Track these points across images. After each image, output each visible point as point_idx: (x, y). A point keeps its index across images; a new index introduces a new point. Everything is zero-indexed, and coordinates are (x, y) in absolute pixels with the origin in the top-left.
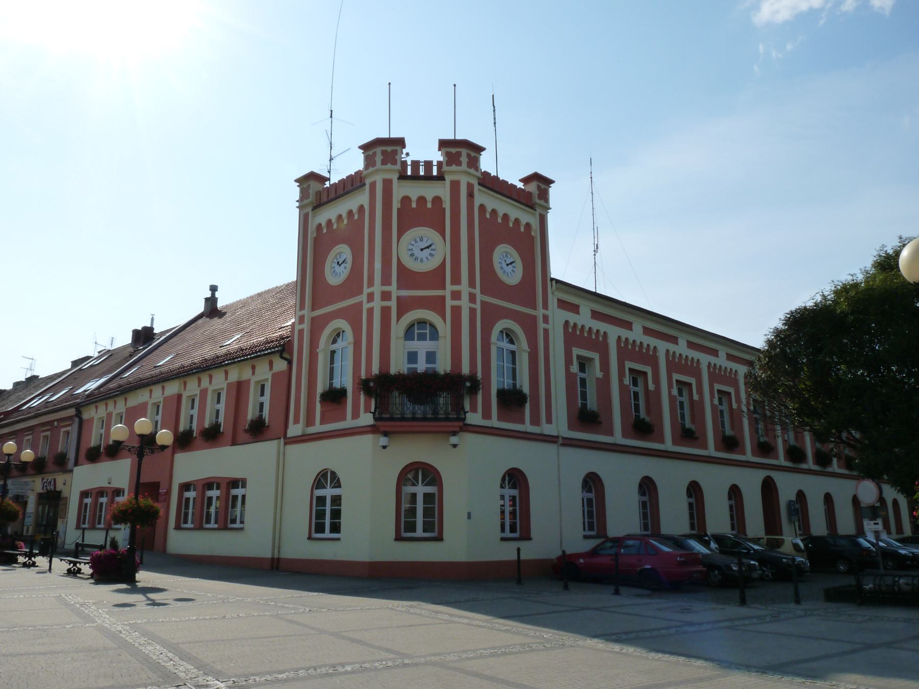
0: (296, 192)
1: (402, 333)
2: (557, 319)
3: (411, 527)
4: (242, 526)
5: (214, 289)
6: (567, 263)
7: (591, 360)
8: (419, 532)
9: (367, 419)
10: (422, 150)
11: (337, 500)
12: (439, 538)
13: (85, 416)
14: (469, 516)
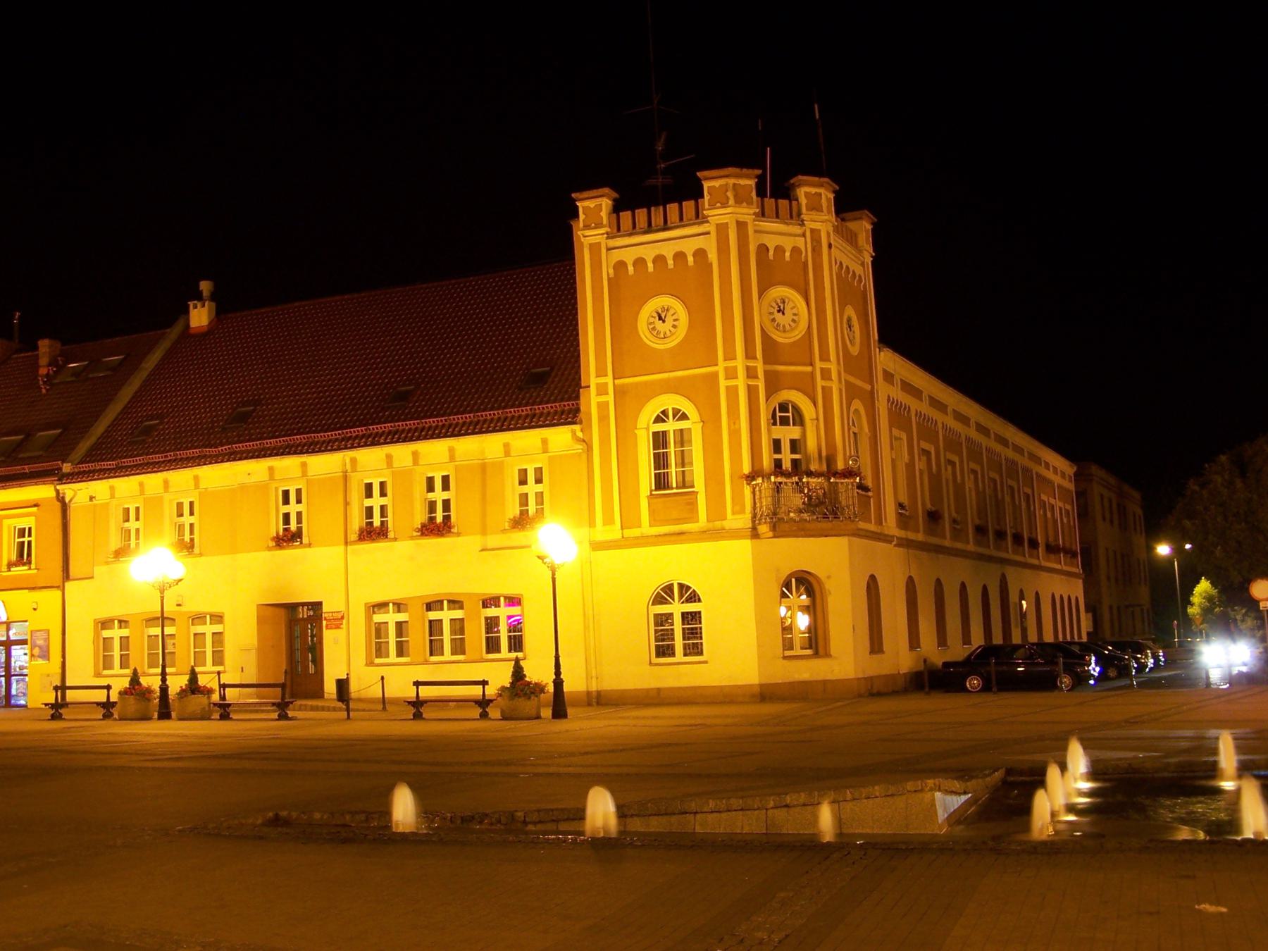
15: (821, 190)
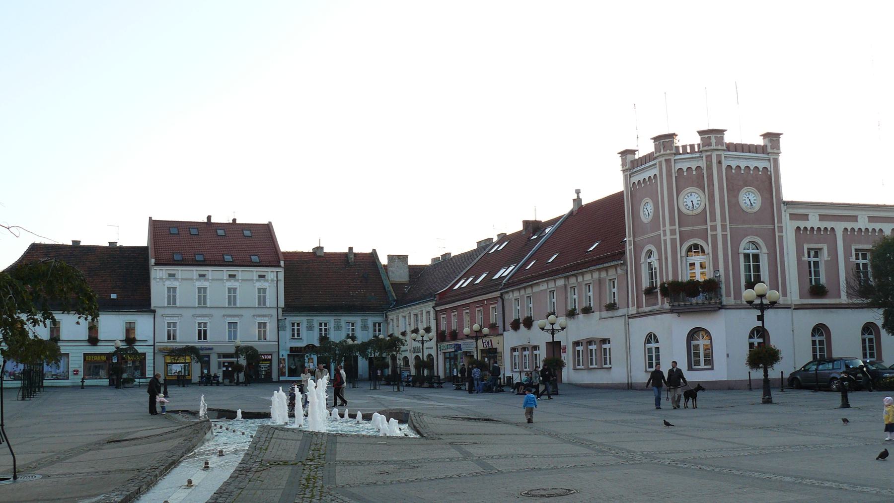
0: (619, 160)
1: (684, 253)
2: (789, 228)
3: (698, 363)
5: (578, 192)
6: (792, 189)
7: (821, 249)
8: (702, 366)
9: (667, 306)
10: (688, 137)
11: (657, 349)
12: (712, 369)
13: (506, 297)
14: (728, 355)
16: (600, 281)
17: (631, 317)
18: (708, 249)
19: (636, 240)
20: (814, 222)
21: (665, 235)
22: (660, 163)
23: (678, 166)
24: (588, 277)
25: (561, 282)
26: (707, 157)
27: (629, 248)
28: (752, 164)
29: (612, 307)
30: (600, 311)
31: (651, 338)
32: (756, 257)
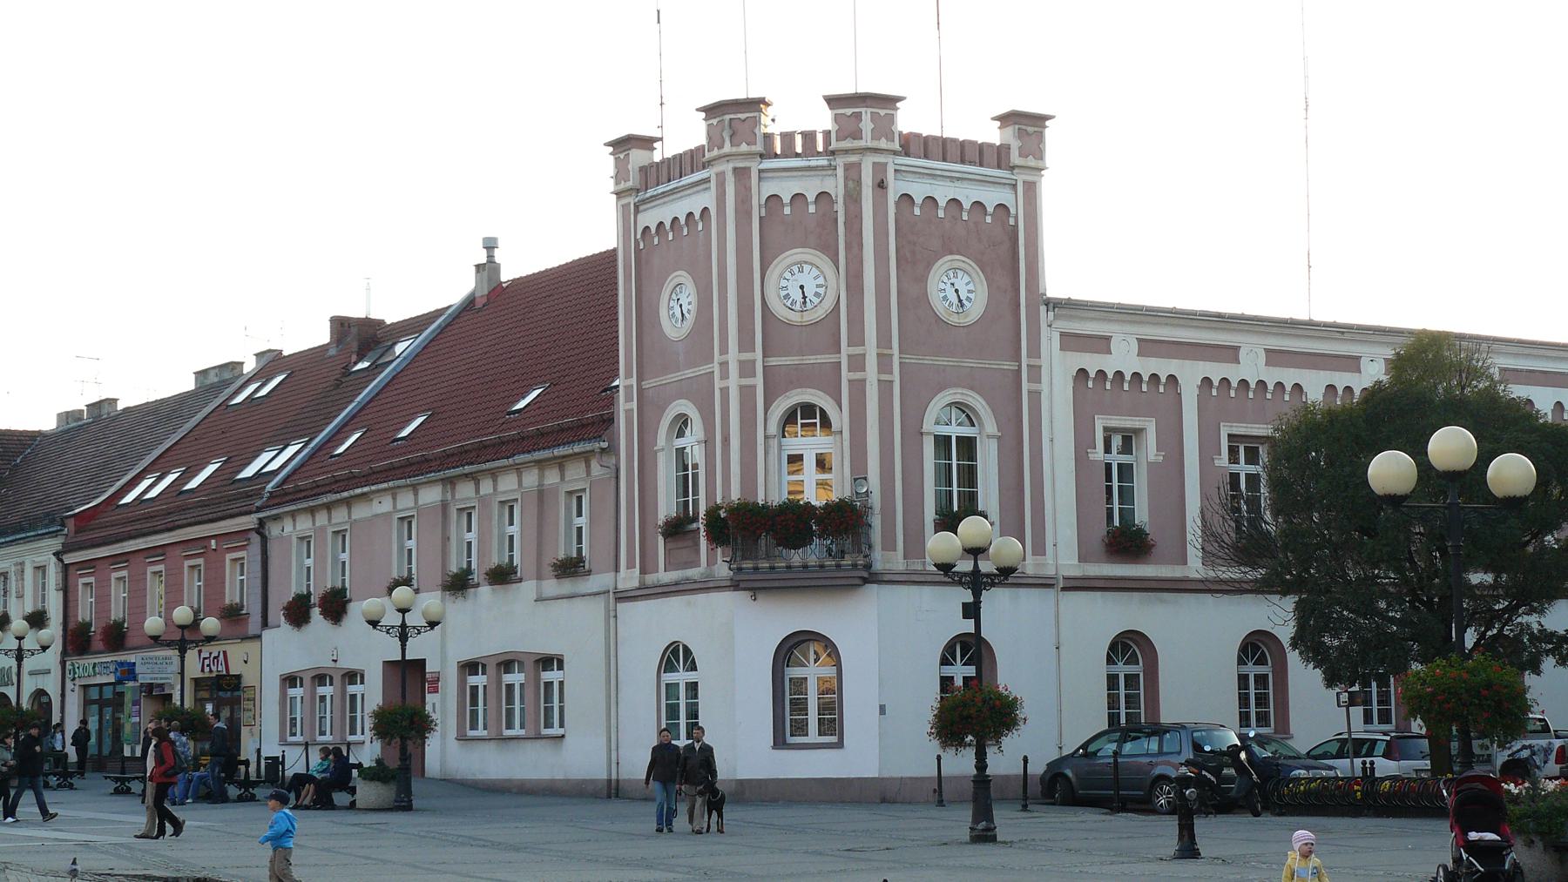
0: (608, 163)
1: (773, 428)
2: (1057, 372)
3: (800, 728)
4: (561, 732)
5: (490, 245)
6: (1071, 266)
7: (1138, 432)
8: (813, 736)
9: (723, 570)
10: (798, 111)
11: (693, 688)
12: (840, 745)
13: (274, 530)
14: (882, 710)
15: (863, 110)
16: (541, 494)
17: (623, 597)
18: (840, 419)
19: (646, 385)
20: (1124, 358)
21: (725, 375)
22: (721, 177)
23: (769, 188)
24: (508, 483)
25: (431, 495)
26: (847, 167)
27: (625, 407)
28: (968, 195)
29: (571, 568)
30: (539, 577)
31: (676, 656)
32: (968, 446)
